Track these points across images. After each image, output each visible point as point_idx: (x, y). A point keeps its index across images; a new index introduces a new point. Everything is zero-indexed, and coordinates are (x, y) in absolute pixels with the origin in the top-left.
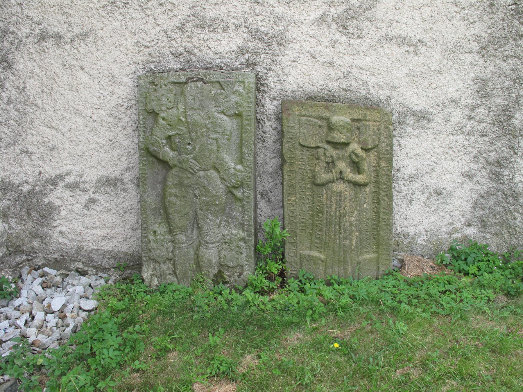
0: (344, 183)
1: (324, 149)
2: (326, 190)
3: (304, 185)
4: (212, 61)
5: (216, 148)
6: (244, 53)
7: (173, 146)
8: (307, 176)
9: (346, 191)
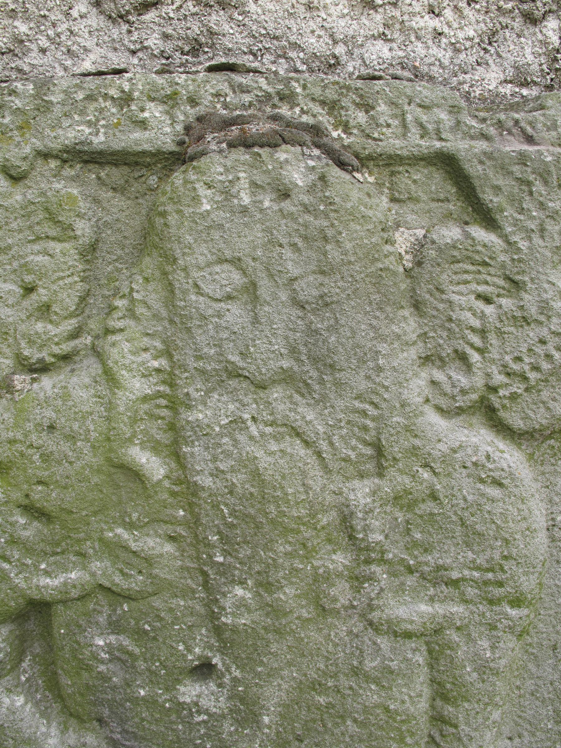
4: (340, 50)
5: (423, 704)
6: (538, 14)
7: (65, 681)
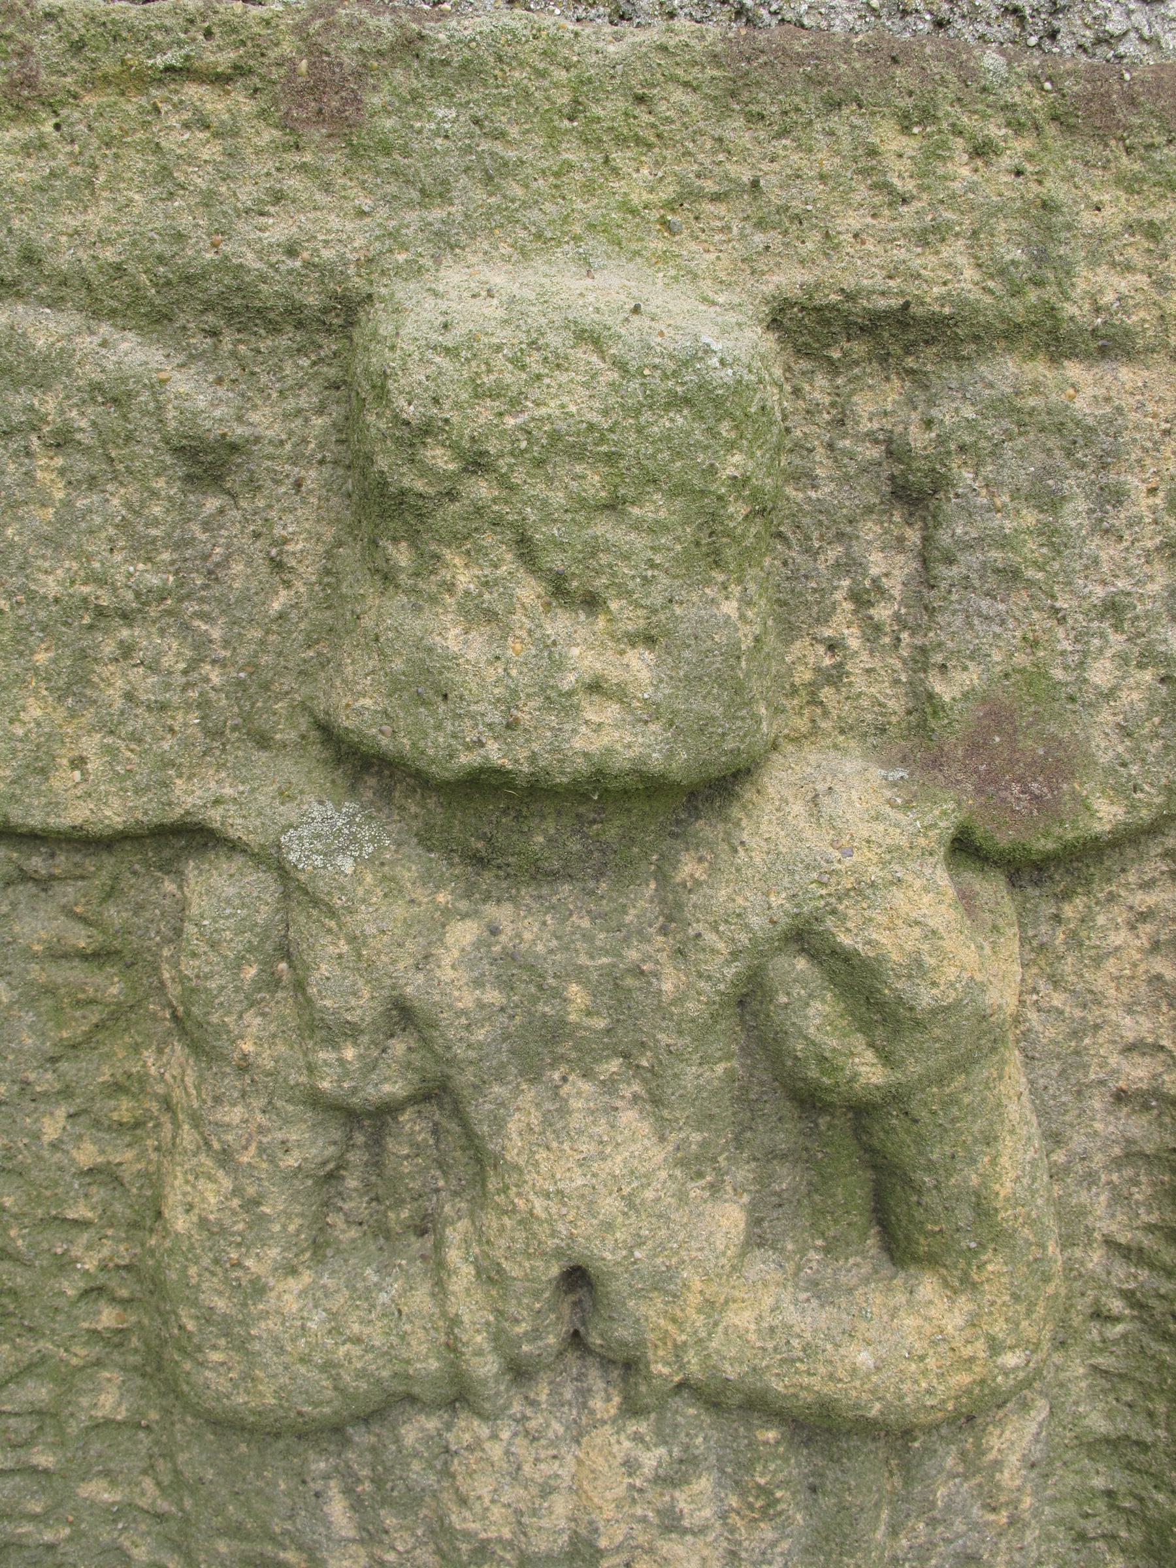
0: (632, 1408)
1: (283, 872)
2: (357, 1504)
3: (39, 1392)
8: (64, 1264)
9: (671, 1523)
